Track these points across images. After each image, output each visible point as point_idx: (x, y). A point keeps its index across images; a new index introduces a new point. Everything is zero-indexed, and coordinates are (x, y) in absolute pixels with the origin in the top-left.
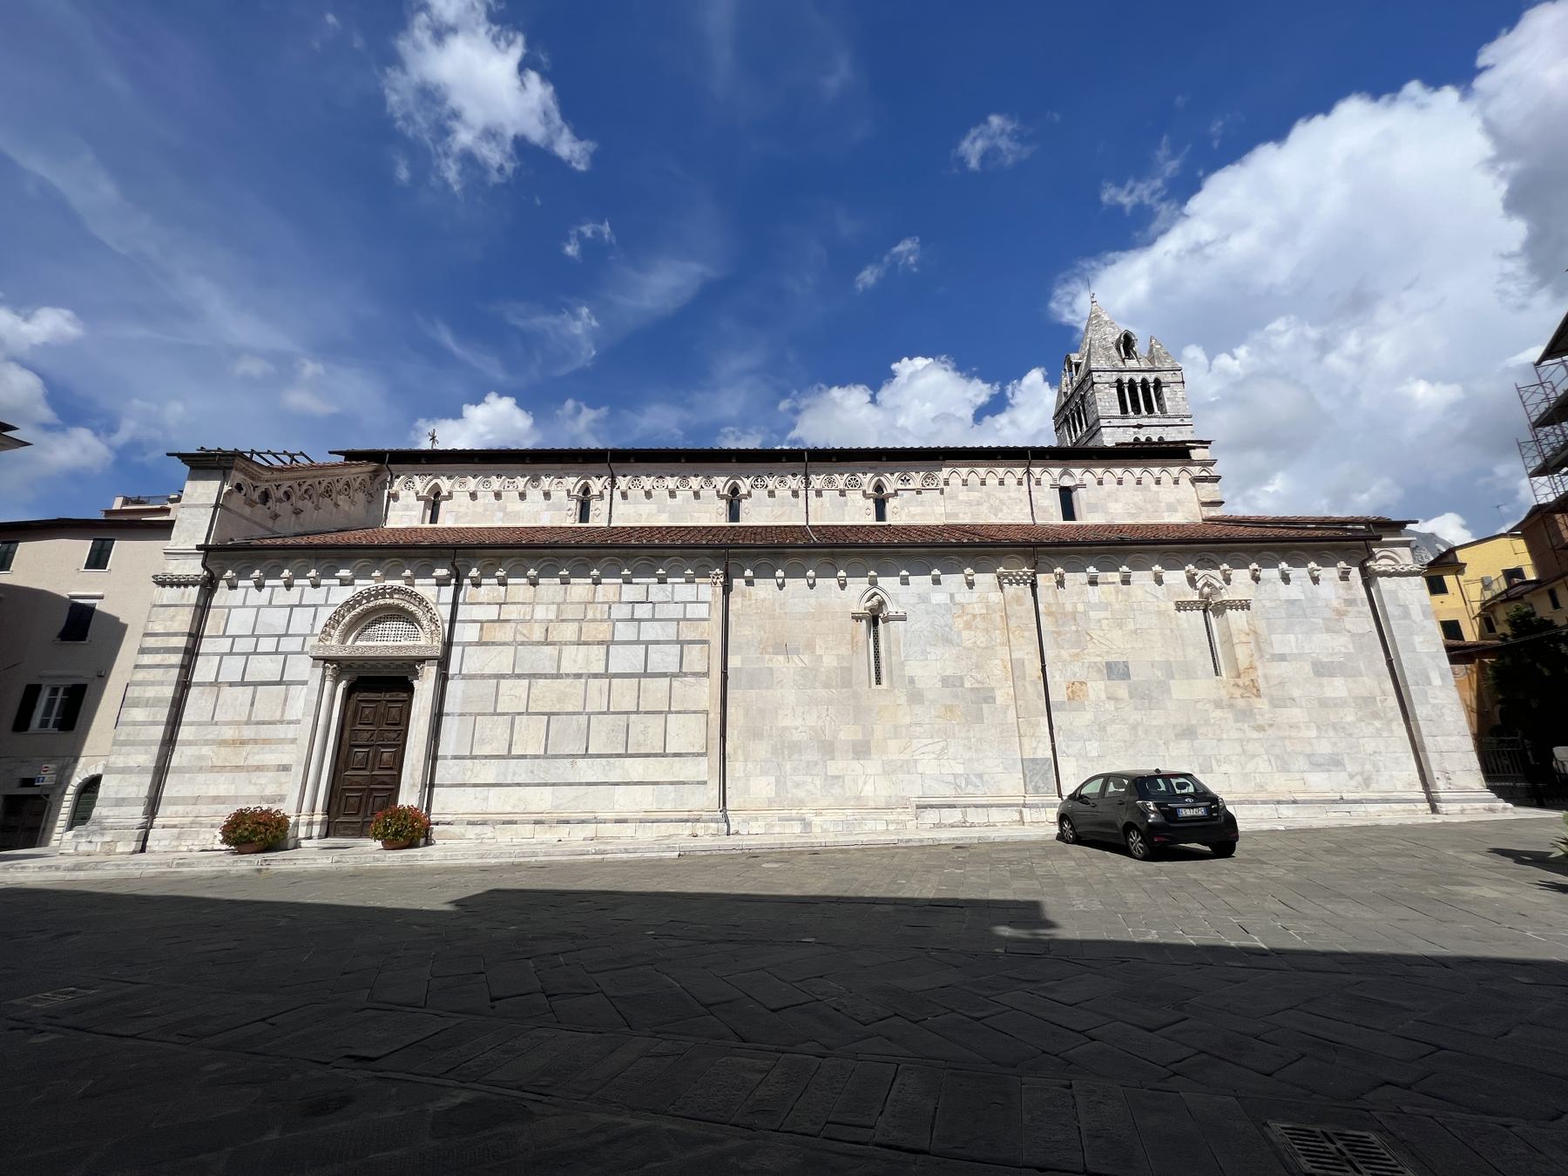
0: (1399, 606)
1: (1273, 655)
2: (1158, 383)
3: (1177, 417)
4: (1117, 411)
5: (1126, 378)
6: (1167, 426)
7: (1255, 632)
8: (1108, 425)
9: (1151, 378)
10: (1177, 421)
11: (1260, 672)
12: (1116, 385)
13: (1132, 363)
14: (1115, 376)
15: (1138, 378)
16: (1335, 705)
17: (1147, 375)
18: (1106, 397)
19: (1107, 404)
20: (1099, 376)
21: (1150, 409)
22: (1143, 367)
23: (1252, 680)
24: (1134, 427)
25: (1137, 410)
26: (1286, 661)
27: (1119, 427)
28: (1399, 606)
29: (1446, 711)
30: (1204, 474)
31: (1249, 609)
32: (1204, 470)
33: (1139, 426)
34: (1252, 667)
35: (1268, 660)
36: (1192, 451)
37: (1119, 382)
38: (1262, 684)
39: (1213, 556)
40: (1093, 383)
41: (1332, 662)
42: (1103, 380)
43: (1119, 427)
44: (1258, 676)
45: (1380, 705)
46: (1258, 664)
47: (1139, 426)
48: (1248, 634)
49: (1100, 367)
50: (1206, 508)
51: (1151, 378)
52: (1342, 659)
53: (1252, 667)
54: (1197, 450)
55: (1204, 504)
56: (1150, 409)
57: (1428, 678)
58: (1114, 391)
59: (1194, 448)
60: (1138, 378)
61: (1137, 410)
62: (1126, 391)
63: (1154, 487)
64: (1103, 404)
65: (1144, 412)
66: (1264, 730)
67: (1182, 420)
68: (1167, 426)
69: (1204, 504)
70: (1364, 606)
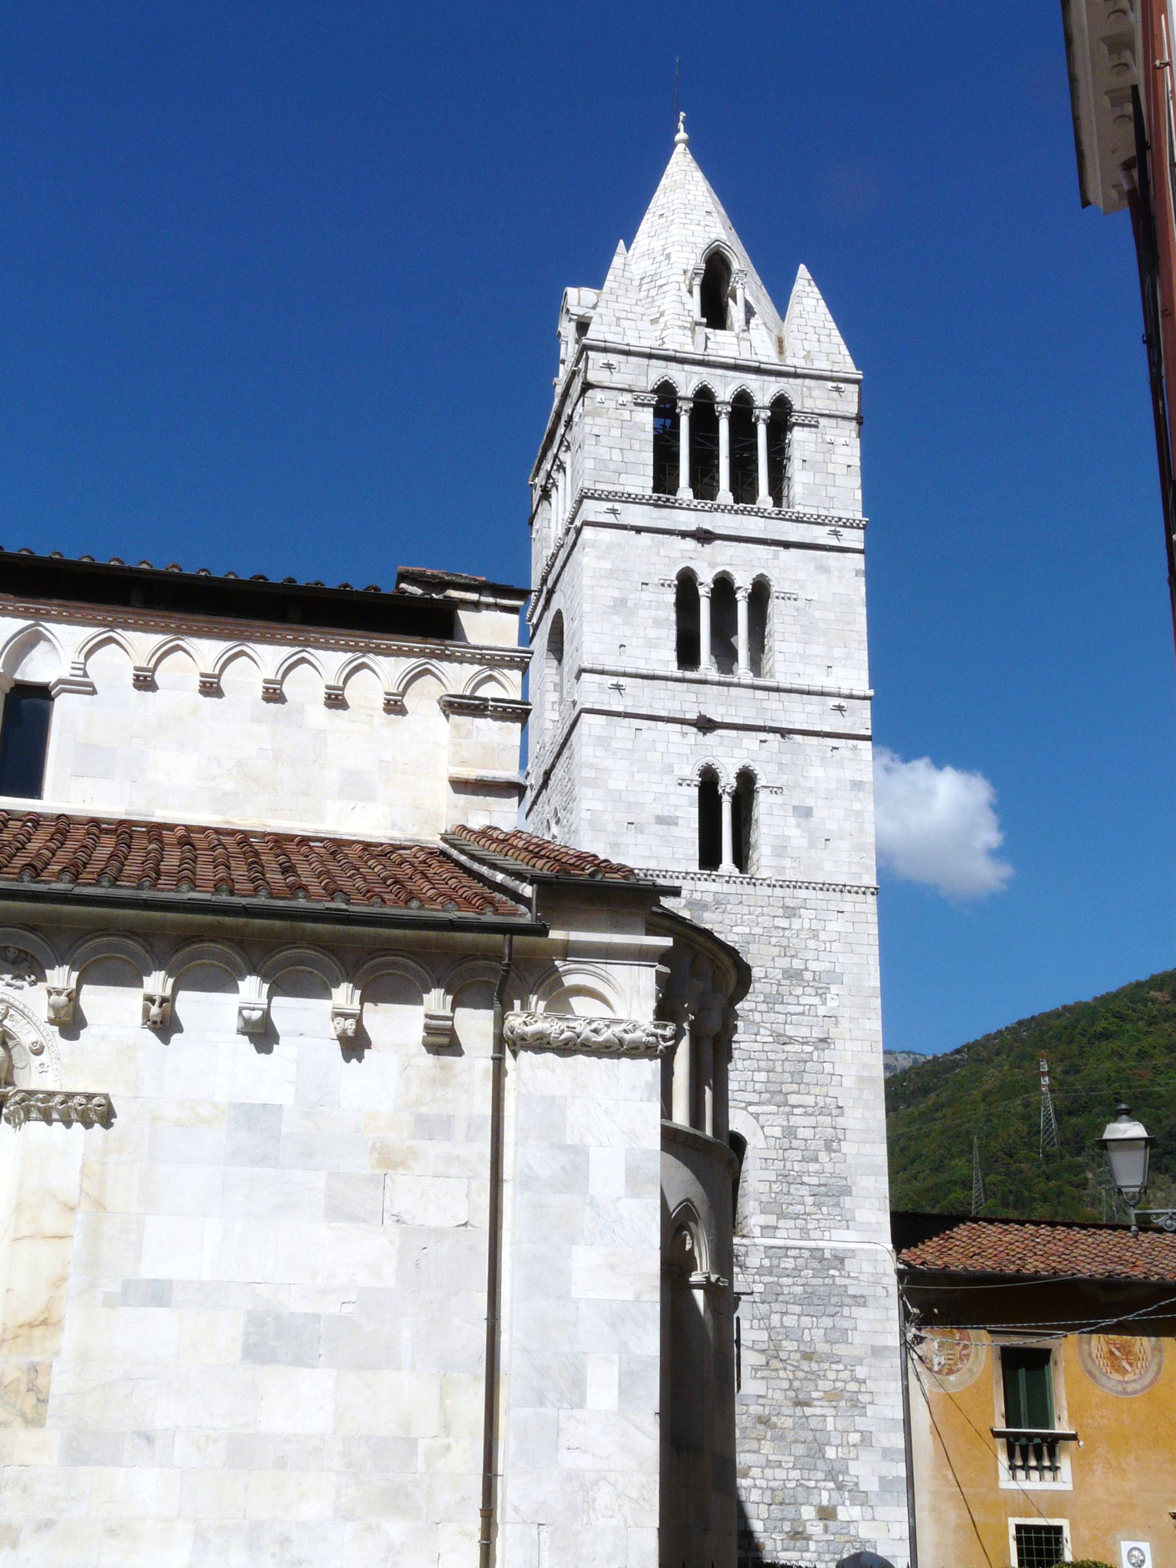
0: (561, 1147)
1: (128, 1284)
2: (781, 406)
3: (819, 522)
4: (642, 481)
5: (686, 383)
6: (787, 545)
7: (100, 1205)
8: (610, 519)
9: (763, 392)
10: (820, 535)
11: (69, 1338)
12: (654, 400)
13: (724, 345)
14: (657, 372)
15: (724, 389)
16: (281, 1463)
17: (752, 383)
18: (616, 432)
19: (616, 455)
20: (609, 366)
21: (744, 489)
22: (745, 356)
23: (34, 1369)
24: (684, 534)
25: (704, 486)
26: (167, 1304)
27: (639, 530)
28: (561, 1147)
29: (603, 1496)
30: (489, 691)
31: (107, 1124)
32: (491, 678)
33: (704, 537)
34: (46, 1322)
35: (111, 1302)
36: (464, 616)
37: (666, 391)
38: (60, 1383)
39: (33, 943)
40: (587, 386)
41: (316, 1317)
42: (617, 380)
43: (639, 530)
44: (57, 1353)
45: (421, 1465)
46: (72, 1315)
47: (704, 537)
48: (72, 1209)
49: (613, 338)
50: (463, 799)
51: (763, 392)
52: (347, 1309)
53: (46, 1322)
54: (485, 613)
55: (461, 786)
56: (744, 489)
57: (578, 1384)
58: (646, 418)
59: (476, 606)
60: (724, 389)
61: (704, 486)
62: (684, 422)
63: (319, 713)
64: (604, 453)
65: (725, 495)
66: (14, 1545)
67: (836, 533)
68: (787, 545)
69: (461, 786)
70: (470, 1138)
